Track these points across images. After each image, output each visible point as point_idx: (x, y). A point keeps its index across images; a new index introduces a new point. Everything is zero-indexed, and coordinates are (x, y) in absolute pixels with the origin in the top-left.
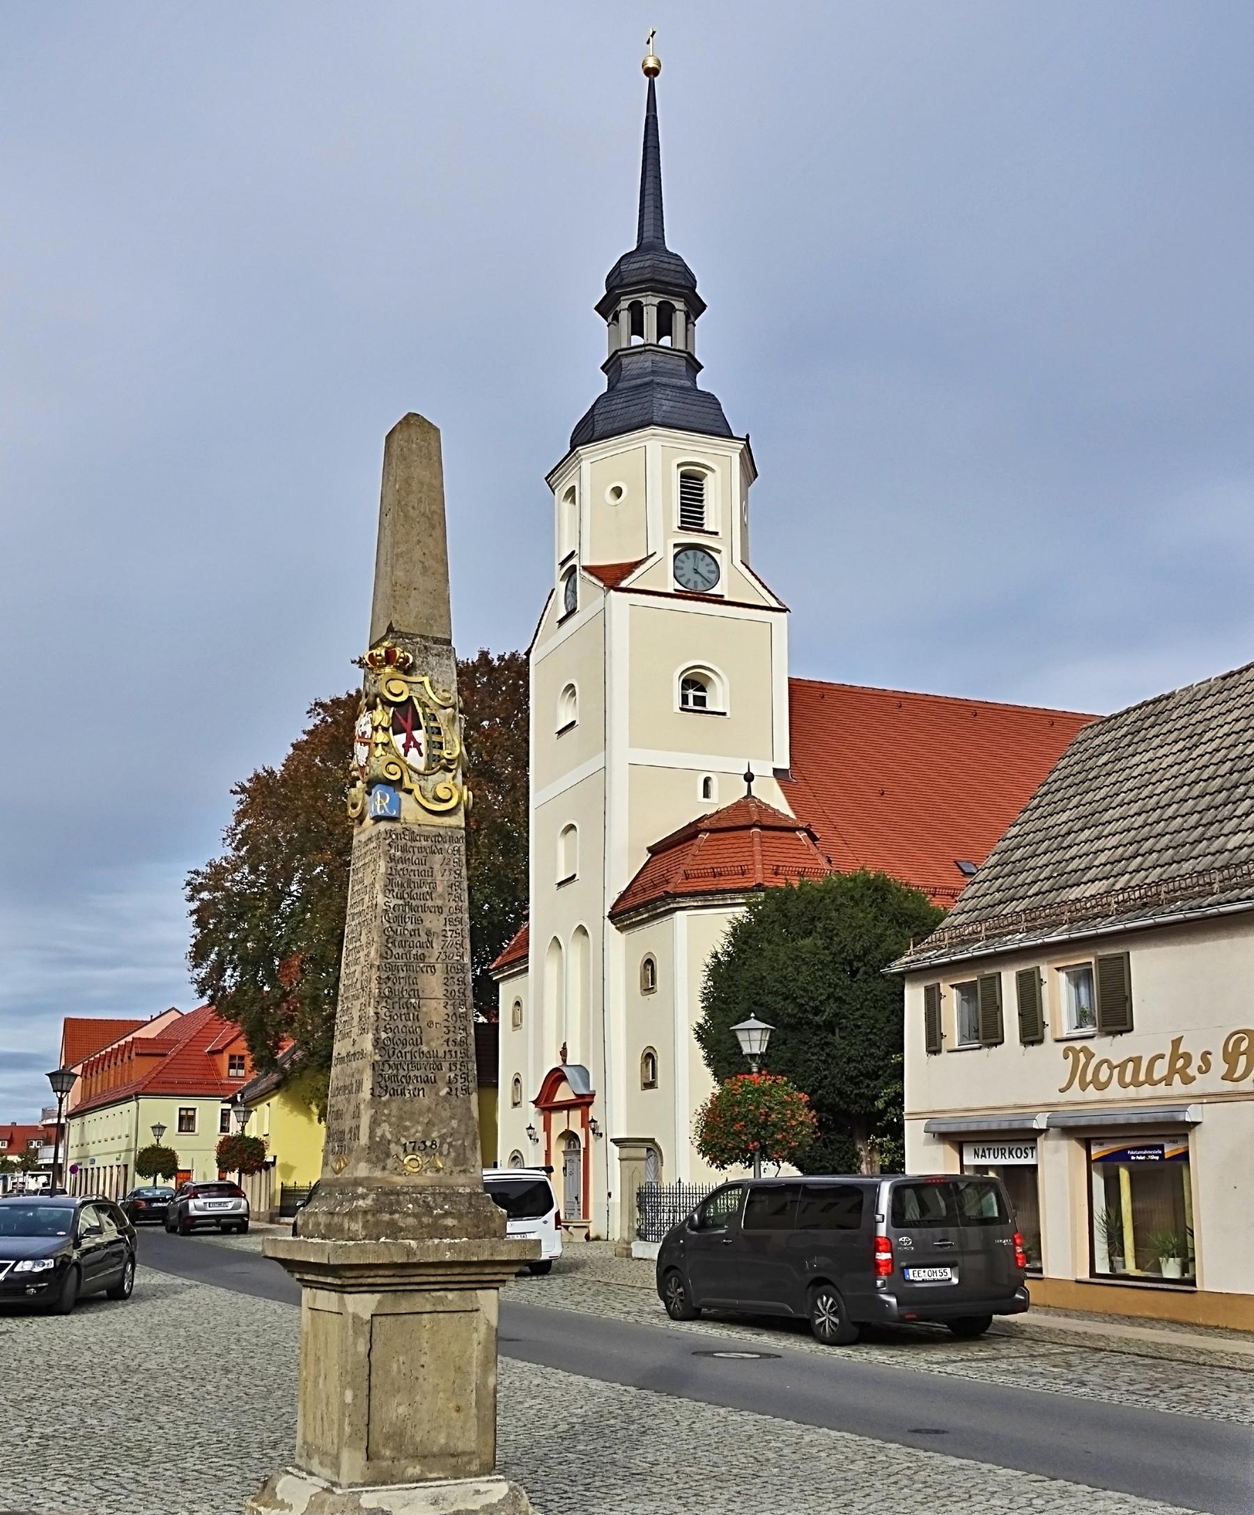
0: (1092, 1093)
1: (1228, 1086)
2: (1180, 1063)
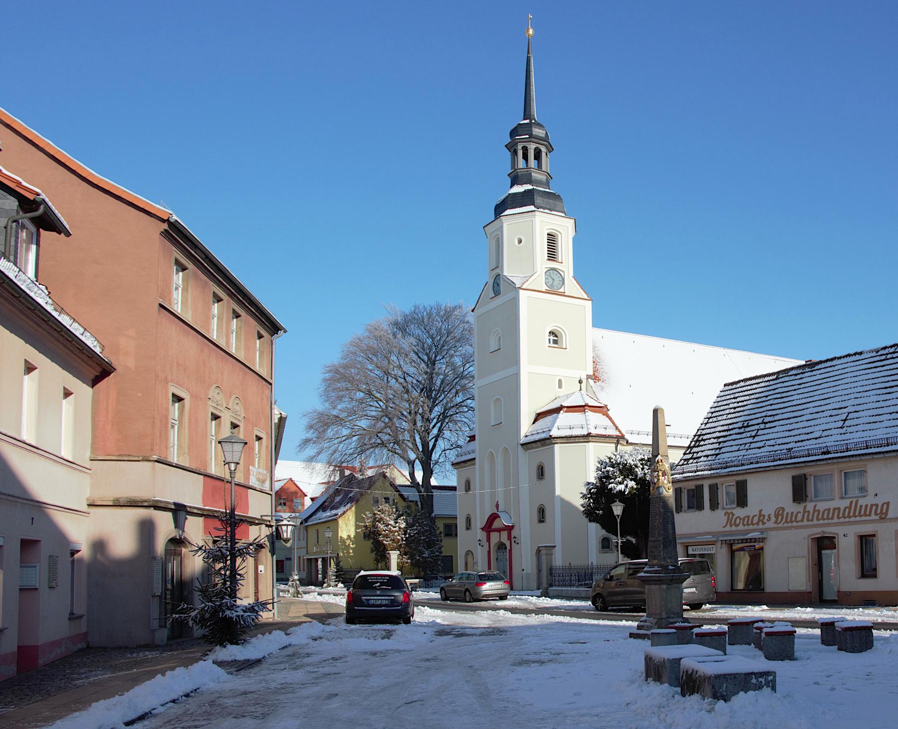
0: (734, 528)
1: (775, 525)
2: (762, 518)
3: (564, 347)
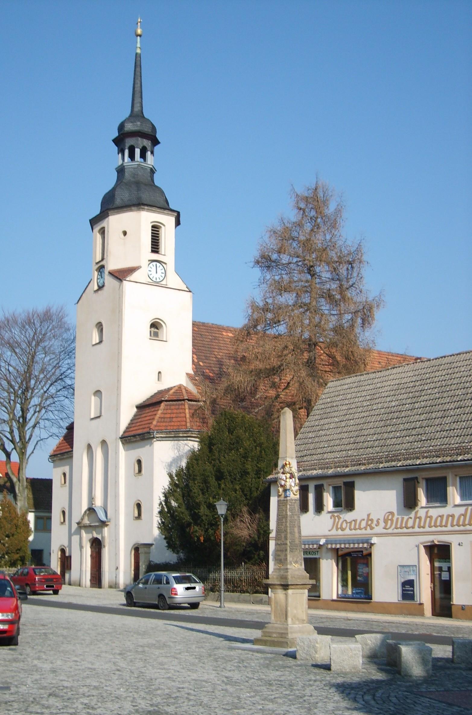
0: (340, 532)
2: (370, 522)
3: (165, 340)
